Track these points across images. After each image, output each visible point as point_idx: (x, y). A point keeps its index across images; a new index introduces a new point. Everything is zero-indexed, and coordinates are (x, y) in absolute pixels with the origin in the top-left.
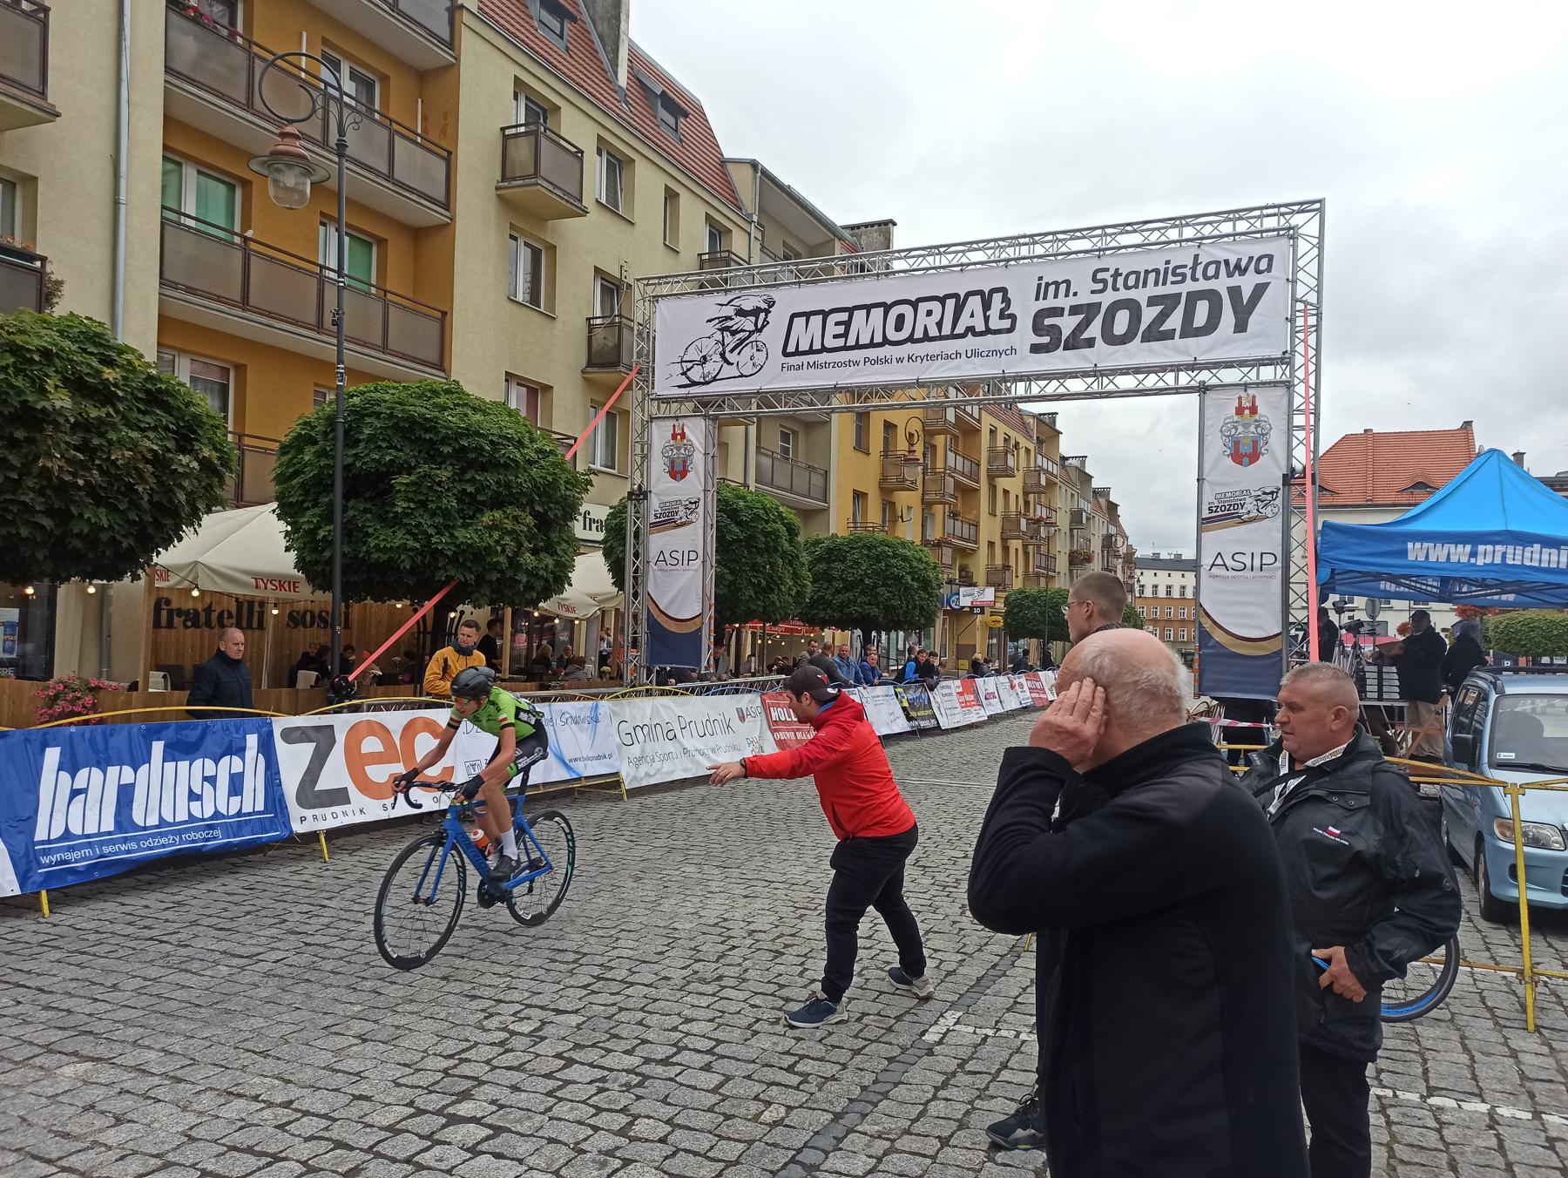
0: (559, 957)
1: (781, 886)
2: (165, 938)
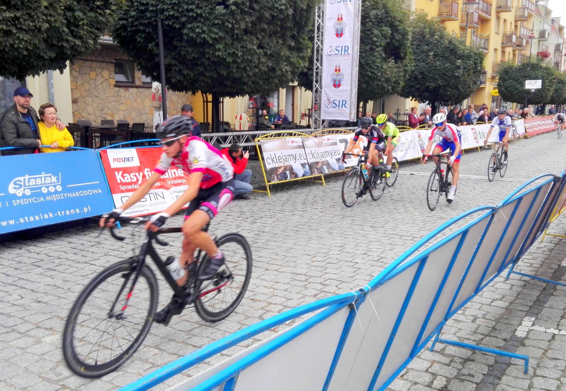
0: (297, 278)
1: (409, 238)
2: (93, 262)
